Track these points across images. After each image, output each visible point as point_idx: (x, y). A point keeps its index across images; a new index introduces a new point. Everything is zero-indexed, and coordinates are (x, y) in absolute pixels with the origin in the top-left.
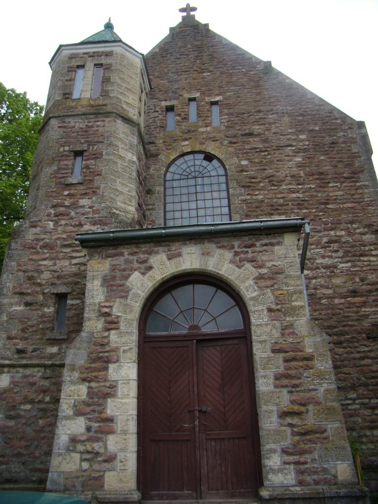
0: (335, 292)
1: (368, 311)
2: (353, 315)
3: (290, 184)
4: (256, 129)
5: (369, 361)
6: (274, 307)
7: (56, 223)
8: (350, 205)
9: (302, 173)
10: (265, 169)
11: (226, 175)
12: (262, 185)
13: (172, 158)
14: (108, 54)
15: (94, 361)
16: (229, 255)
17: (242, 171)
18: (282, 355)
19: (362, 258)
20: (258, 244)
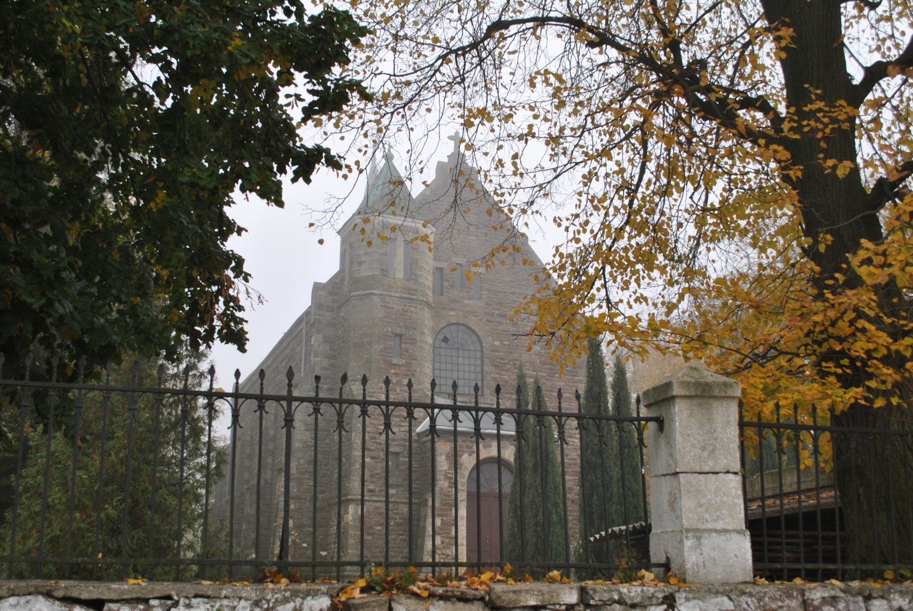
11: (482, 351)
13: (442, 326)
15: (444, 505)
17: (495, 351)
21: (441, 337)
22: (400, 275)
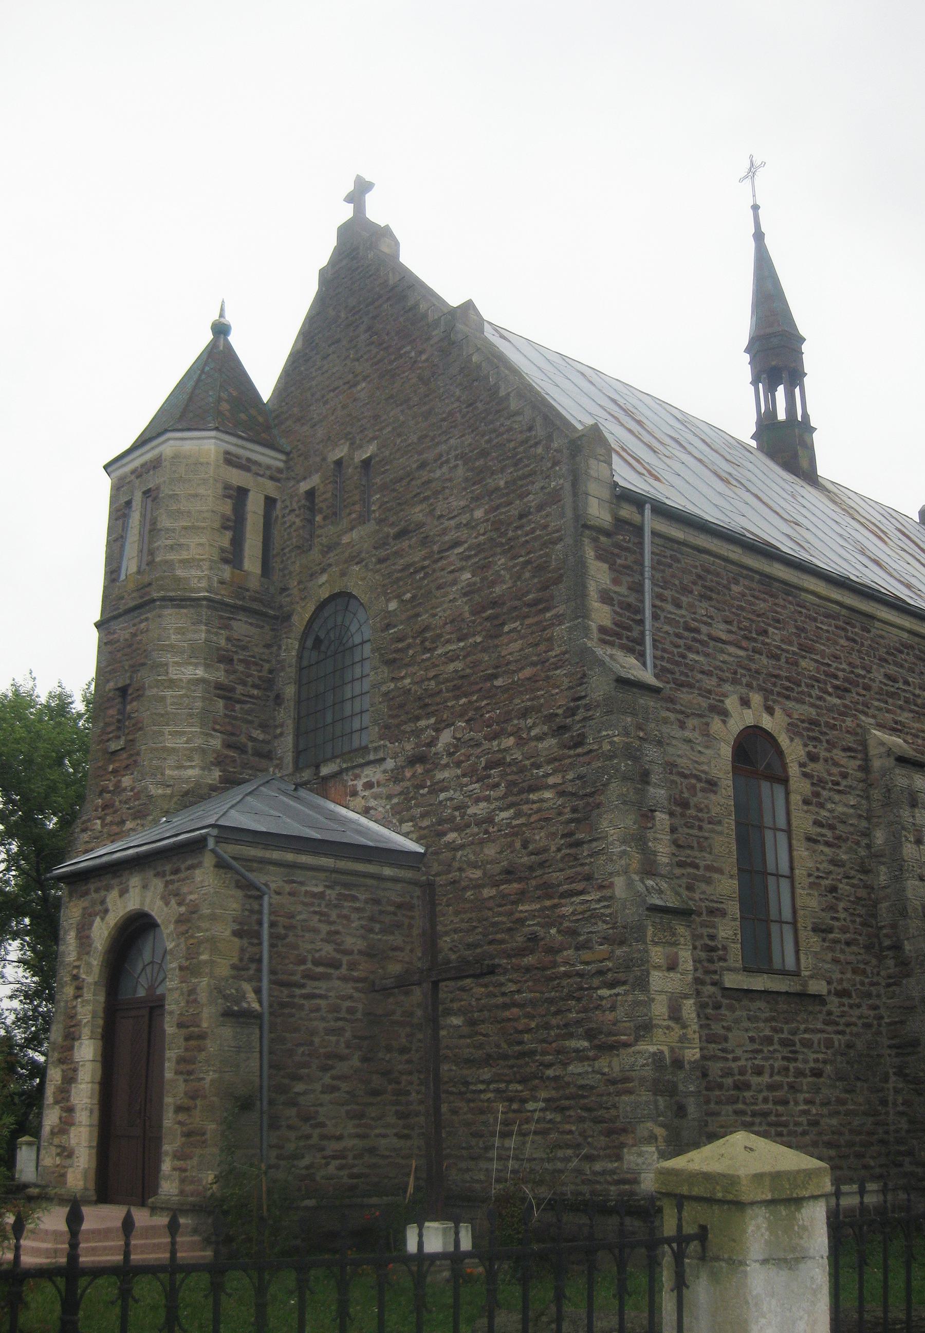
0: (485, 874)
1: (526, 911)
2: (504, 919)
3: (448, 641)
4: (417, 513)
5: (515, 1010)
6: (186, 963)
8: (528, 672)
10: (418, 615)
12: (411, 652)
13: (307, 616)
16: (158, 885)
17: (388, 626)
18: (184, 1031)
19: (531, 796)
20: (183, 867)
21: (309, 643)
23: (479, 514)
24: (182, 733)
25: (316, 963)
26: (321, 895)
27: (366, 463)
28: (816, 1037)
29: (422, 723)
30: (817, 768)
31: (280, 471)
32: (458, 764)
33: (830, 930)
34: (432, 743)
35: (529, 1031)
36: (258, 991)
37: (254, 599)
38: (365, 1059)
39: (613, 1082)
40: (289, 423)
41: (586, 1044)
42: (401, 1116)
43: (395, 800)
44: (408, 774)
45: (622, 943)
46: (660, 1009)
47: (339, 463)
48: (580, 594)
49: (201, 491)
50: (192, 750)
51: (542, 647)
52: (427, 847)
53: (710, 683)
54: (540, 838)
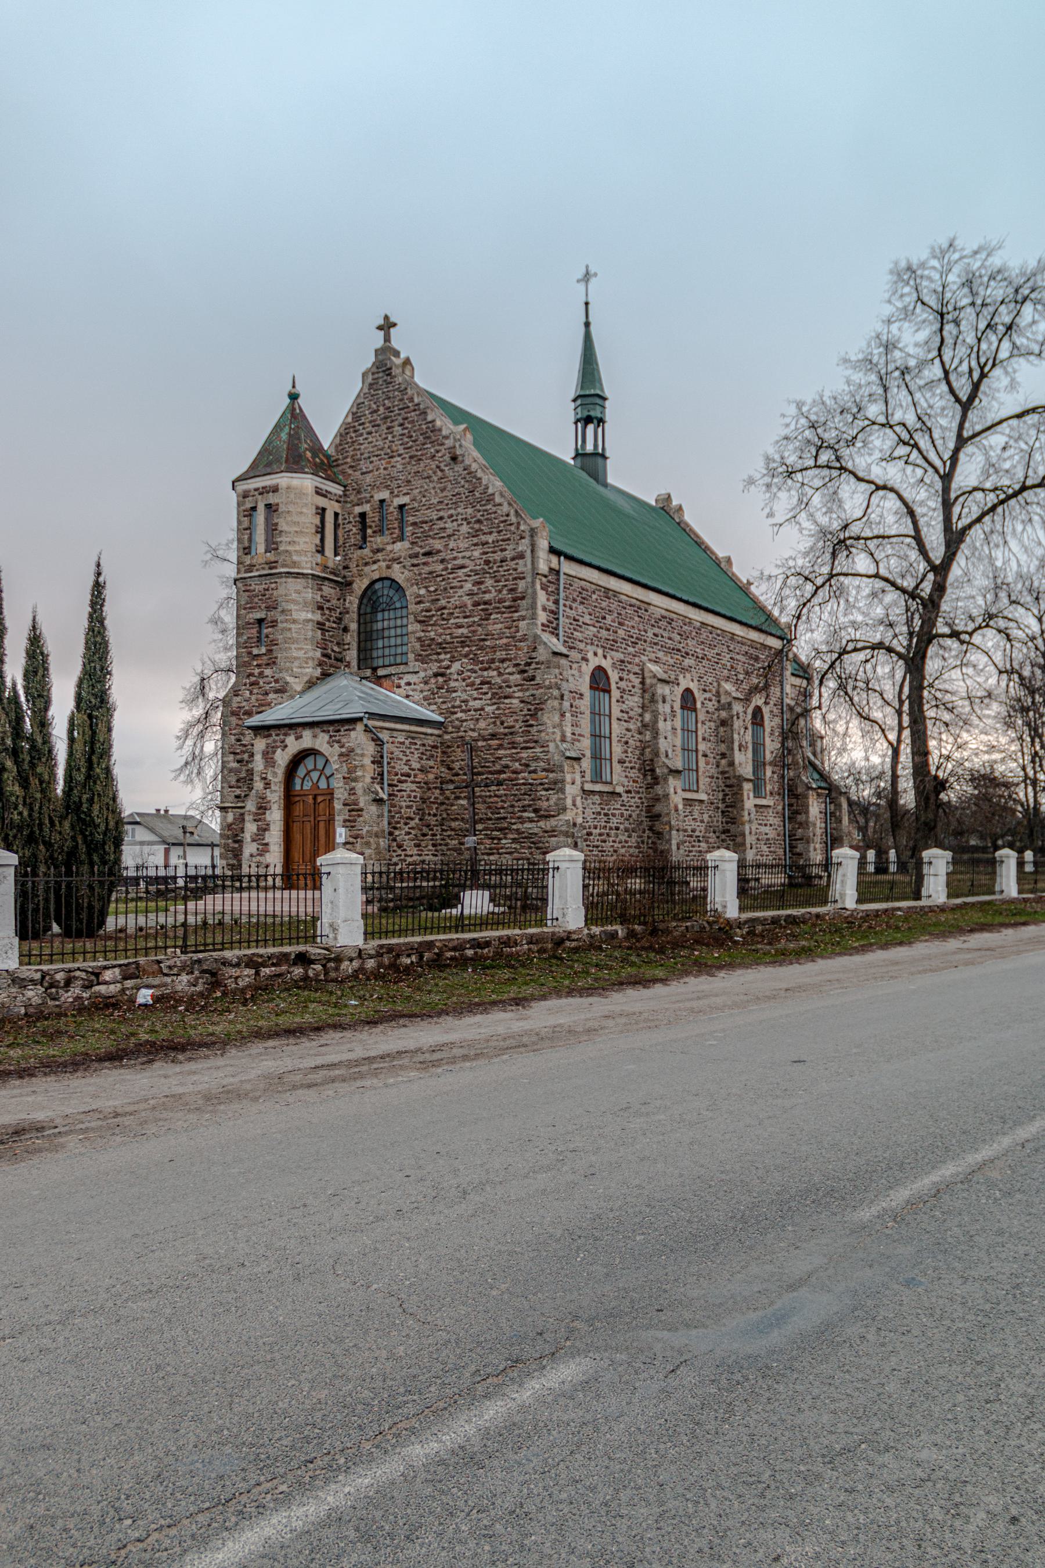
4: (438, 545)
7: (251, 693)
8: (505, 641)
9: (469, 603)
10: (438, 600)
13: (364, 587)
14: (275, 489)
15: (260, 808)
16: (326, 737)
22: (261, 549)
23: (476, 554)
24: (301, 649)
25: (402, 775)
26: (403, 743)
27: (401, 507)
28: (617, 812)
29: (442, 657)
30: (623, 684)
31: (340, 496)
32: (464, 680)
33: (624, 762)
34: (448, 667)
35: (503, 808)
36: (382, 789)
37: (331, 573)
38: (420, 820)
39: (546, 832)
40: (344, 467)
41: (533, 815)
42: (434, 845)
43: (425, 693)
44: (433, 681)
45: (553, 772)
46: (569, 802)
47: (382, 501)
48: (533, 606)
49: (304, 510)
50: (308, 658)
51: (513, 630)
52: (446, 718)
53: (582, 646)
54: (510, 721)
